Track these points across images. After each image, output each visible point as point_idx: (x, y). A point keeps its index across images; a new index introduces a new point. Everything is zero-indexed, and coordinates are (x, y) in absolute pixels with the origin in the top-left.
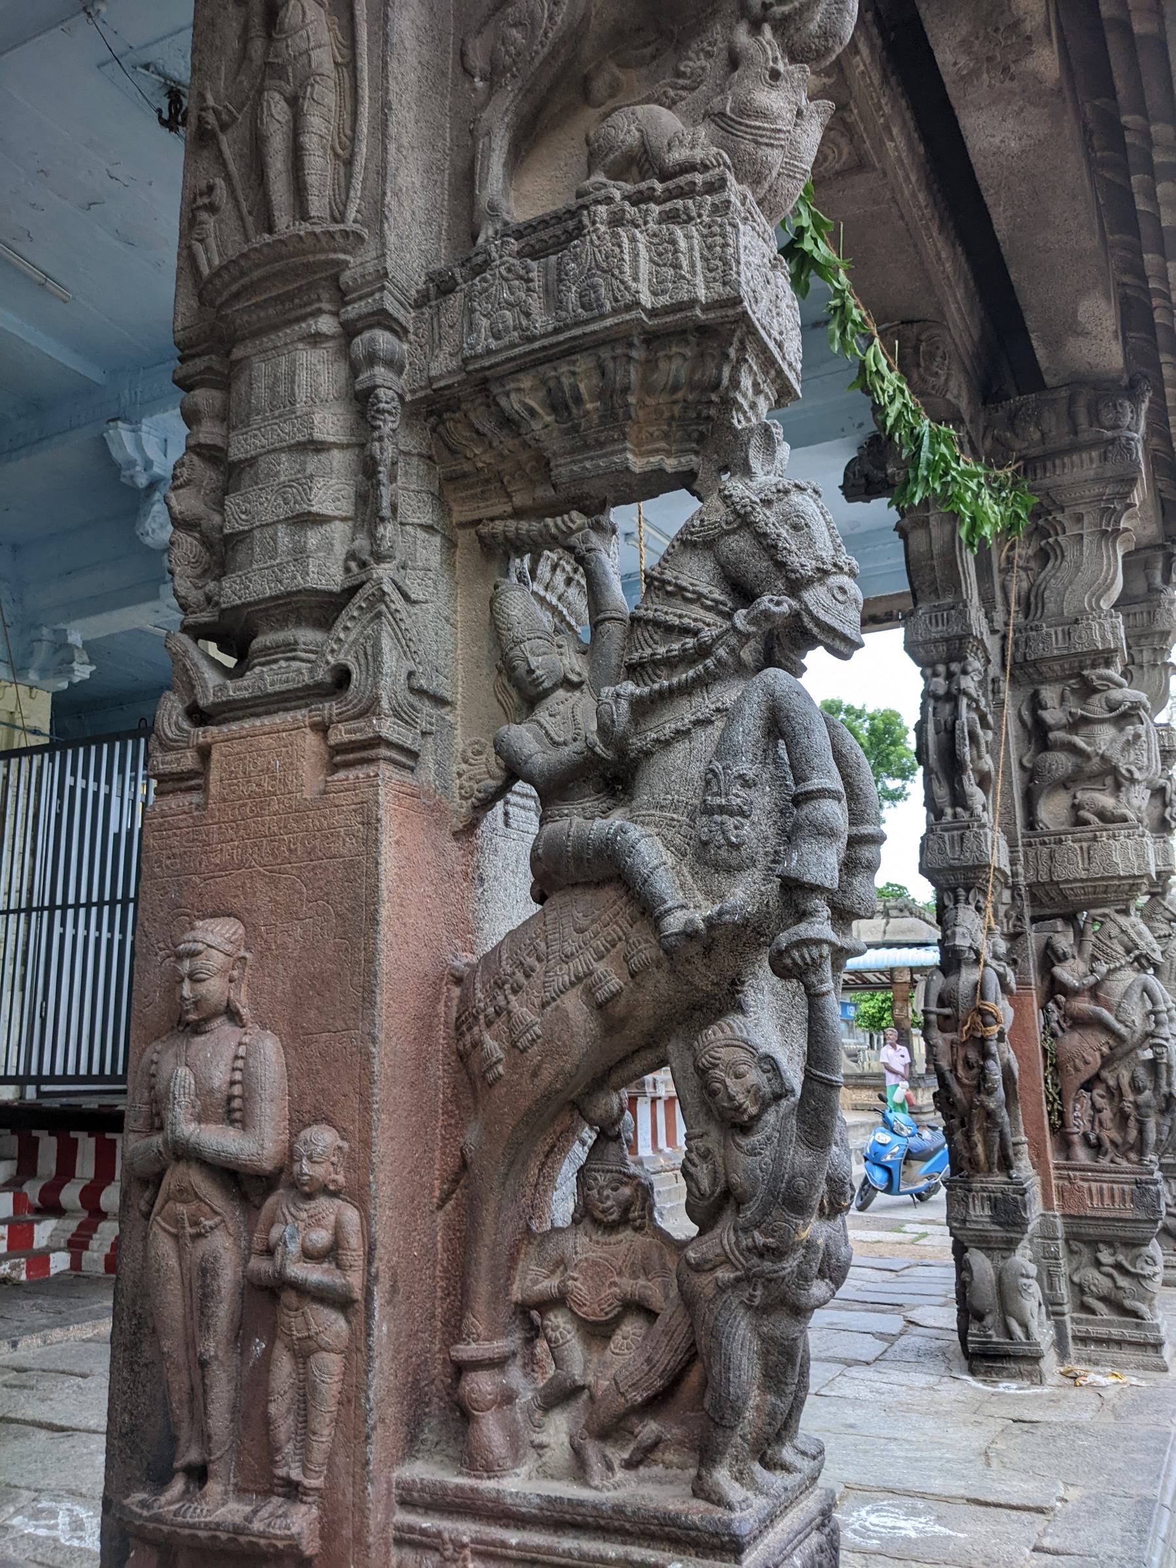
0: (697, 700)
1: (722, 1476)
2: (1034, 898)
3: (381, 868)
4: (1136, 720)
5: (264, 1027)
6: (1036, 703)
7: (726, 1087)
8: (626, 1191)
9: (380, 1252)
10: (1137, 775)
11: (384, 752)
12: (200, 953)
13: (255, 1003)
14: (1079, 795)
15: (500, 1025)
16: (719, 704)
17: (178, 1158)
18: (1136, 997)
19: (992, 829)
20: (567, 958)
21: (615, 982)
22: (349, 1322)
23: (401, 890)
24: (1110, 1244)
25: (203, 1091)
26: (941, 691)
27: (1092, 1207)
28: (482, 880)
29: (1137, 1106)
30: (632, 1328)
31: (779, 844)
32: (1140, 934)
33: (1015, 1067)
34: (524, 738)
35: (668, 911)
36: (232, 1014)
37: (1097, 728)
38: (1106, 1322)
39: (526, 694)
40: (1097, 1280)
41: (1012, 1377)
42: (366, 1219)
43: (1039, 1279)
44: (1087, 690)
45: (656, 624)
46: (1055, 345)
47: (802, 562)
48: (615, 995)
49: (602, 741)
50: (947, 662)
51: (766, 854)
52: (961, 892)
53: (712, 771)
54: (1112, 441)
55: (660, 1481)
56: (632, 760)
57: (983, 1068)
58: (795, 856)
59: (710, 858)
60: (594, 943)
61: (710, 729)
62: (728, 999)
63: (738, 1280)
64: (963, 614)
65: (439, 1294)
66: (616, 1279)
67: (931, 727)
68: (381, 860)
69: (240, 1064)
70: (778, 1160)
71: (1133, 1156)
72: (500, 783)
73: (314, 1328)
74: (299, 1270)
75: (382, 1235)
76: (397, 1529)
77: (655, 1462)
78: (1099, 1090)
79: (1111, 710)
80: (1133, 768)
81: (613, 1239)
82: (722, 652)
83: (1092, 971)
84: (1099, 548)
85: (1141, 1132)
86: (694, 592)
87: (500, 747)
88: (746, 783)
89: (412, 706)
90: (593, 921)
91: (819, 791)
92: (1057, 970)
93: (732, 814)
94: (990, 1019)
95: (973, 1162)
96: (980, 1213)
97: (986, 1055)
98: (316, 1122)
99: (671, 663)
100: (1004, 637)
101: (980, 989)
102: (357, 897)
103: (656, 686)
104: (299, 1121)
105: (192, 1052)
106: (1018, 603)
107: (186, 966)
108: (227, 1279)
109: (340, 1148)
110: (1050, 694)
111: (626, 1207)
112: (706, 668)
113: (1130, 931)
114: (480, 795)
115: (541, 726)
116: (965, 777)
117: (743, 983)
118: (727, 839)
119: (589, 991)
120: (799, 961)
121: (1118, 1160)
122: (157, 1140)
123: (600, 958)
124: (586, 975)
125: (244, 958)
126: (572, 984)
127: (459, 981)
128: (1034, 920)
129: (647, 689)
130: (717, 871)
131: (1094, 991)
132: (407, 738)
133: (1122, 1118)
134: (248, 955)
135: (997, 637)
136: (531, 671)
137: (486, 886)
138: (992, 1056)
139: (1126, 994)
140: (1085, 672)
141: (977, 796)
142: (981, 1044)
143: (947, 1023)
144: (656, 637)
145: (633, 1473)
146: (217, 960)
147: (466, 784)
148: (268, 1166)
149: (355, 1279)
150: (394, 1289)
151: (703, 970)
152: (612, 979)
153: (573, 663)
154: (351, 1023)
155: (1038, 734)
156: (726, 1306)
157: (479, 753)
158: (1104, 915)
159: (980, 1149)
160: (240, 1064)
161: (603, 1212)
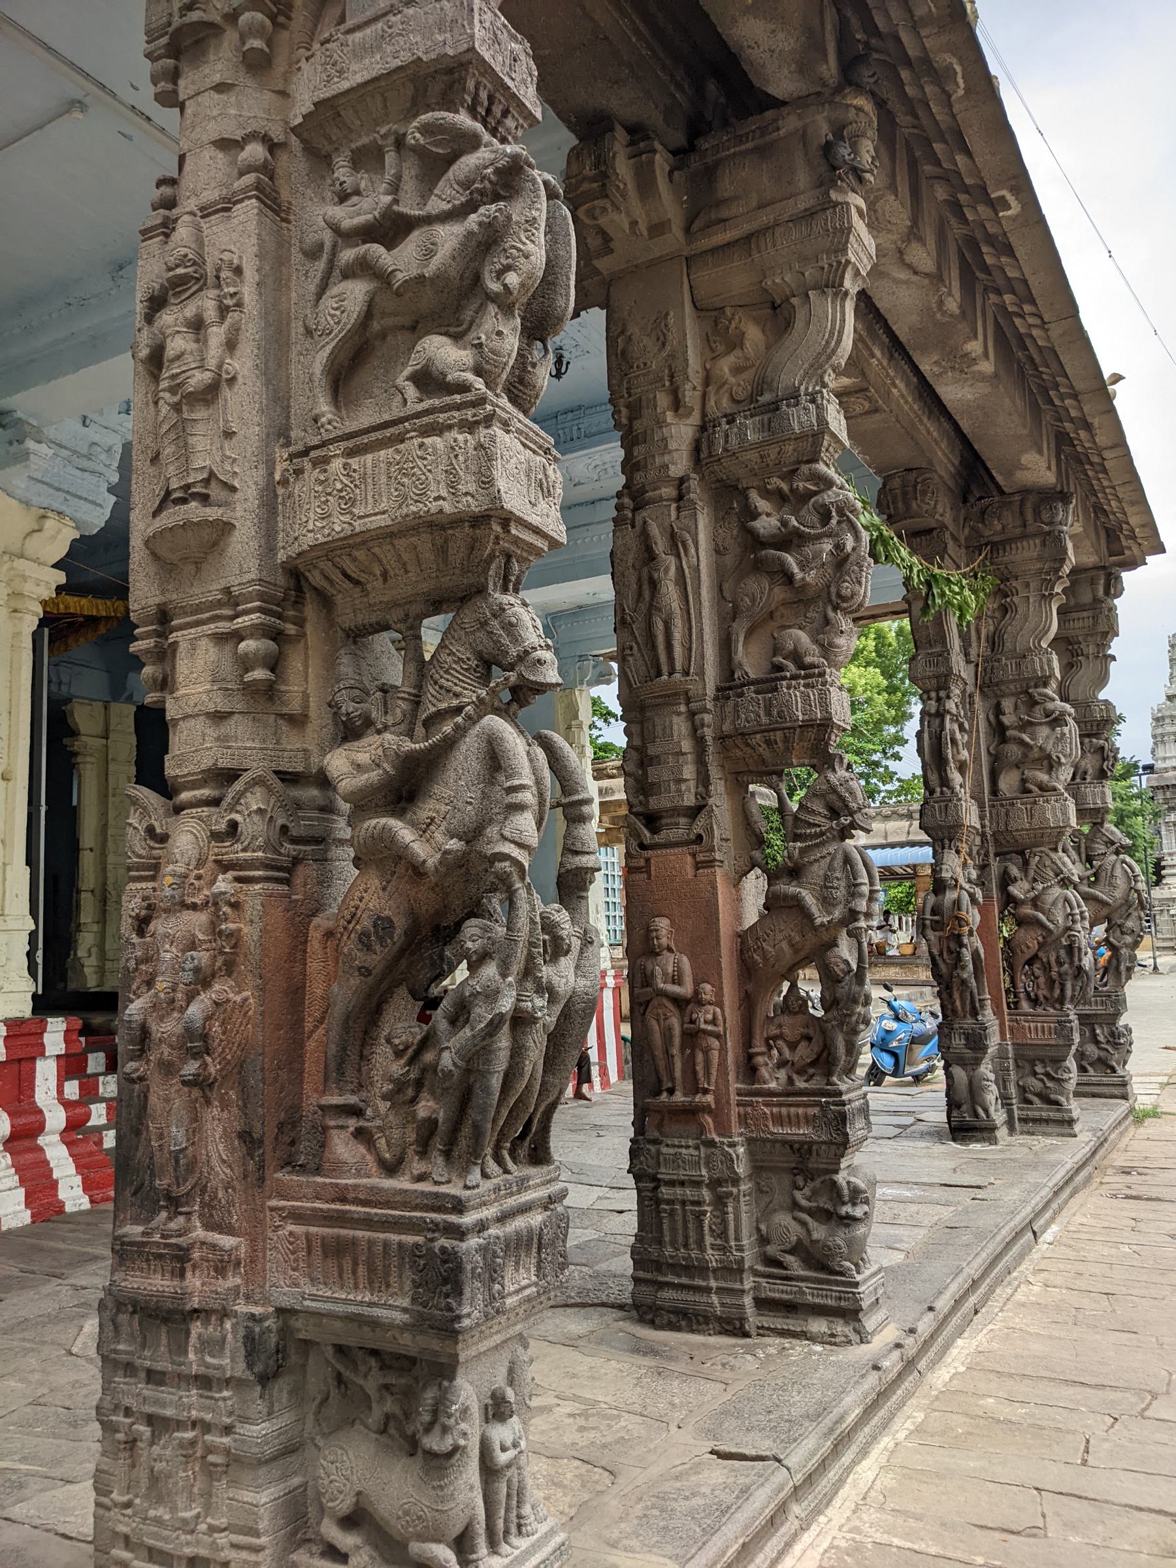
2: (996, 841)
6: (998, 711)
18: (1060, 905)
24: (1042, 1061)
26: (933, 711)
27: (1032, 1038)
29: (1060, 974)
32: (1064, 864)
33: (982, 951)
36: (670, 949)
37: (1038, 728)
38: (1039, 1109)
40: (1034, 1083)
41: (978, 1141)
46: (1009, 474)
47: (853, 805)
50: (937, 690)
52: (947, 842)
57: (959, 953)
59: (827, 902)
62: (834, 944)
64: (947, 660)
67: (926, 735)
74: (703, 1026)
78: (1037, 965)
85: (1062, 990)
92: (1011, 888)
95: (954, 1011)
96: (958, 1042)
97: (961, 945)
101: (957, 903)
104: (697, 983)
108: (677, 1031)
122: (649, 989)
128: (996, 855)
131: (1035, 902)
133: (1051, 983)
139: (1054, 903)
141: (956, 777)
142: (958, 938)
143: (937, 926)
146: (664, 932)
149: (721, 1029)
155: (999, 731)
159: (958, 1003)
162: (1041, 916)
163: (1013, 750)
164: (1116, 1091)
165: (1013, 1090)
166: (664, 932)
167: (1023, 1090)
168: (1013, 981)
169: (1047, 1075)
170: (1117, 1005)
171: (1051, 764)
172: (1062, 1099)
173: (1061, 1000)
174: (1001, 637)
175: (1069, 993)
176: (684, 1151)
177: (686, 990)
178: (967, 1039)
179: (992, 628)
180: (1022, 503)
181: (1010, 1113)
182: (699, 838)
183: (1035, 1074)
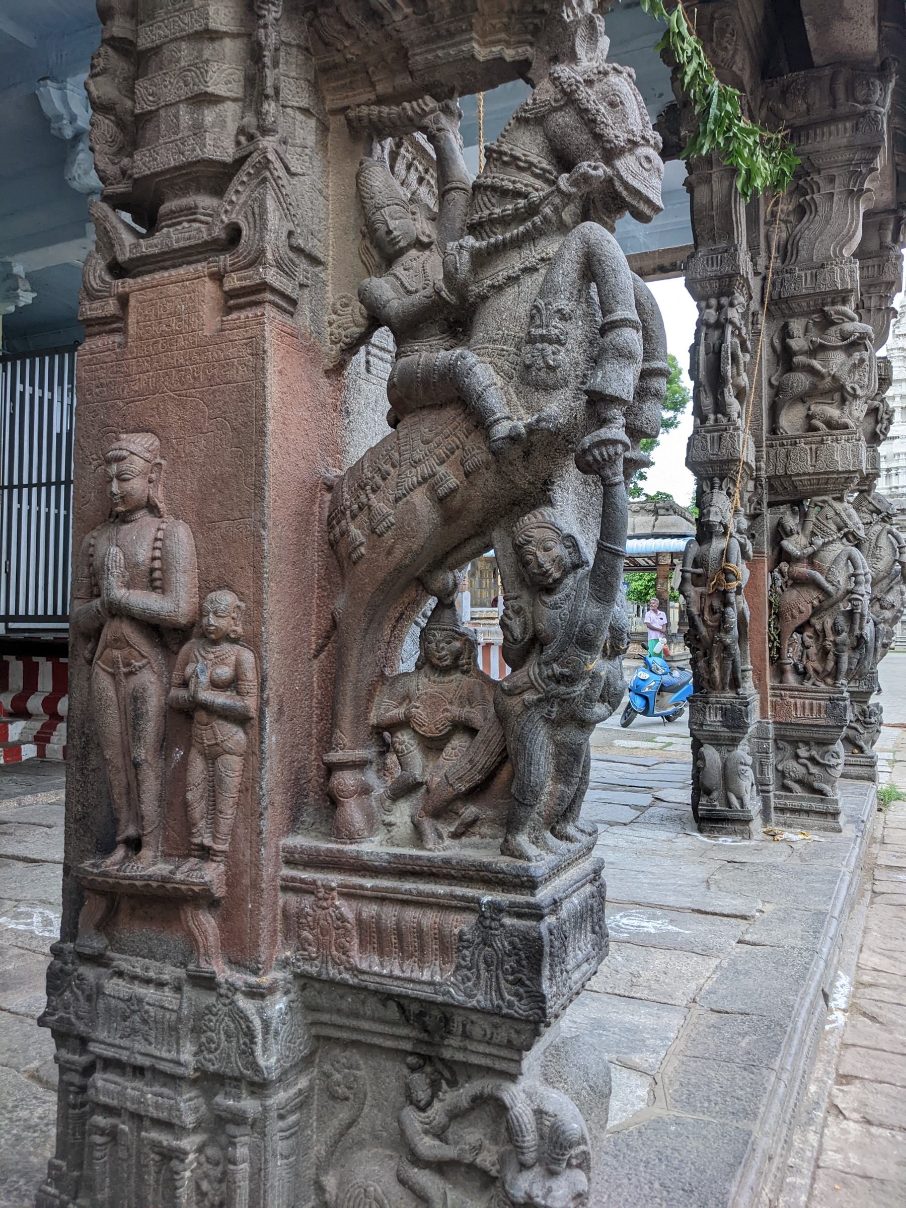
0: (525, 252)
1: (523, 840)
2: (771, 487)
3: (268, 391)
4: (862, 347)
5: (177, 517)
6: (785, 333)
7: (537, 558)
8: (457, 644)
9: (270, 683)
10: (859, 392)
11: (268, 296)
12: (125, 458)
13: (169, 500)
14: (812, 407)
15: (363, 517)
16: (544, 255)
17: (113, 616)
18: (842, 564)
19: (744, 432)
20: (416, 463)
21: (453, 481)
22: (246, 733)
23: (283, 411)
25: (131, 564)
26: (712, 320)
27: (797, 716)
28: (348, 412)
29: (835, 644)
30: (459, 742)
31: (587, 369)
32: (849, 516)
33: (748, 614)
34: (383, 288)
35: (497, 421)
36: (152, 508)
37: (832, 354)
39: (385, 252)
42: (259, 658)
44: (827, 322)
45: (494, 189)
47: (616, 134)
48: (453, 491)
49: (447, 287)
50: (718, 296)
51: (577, 376)
52: (717, 480)
53: (536, 307)
55: (476, 846)
56: (471, 305)
57: (723, 614)
58: (600, 374)
59: (532, 379)
60: (437, 451)
61: (535, 276)
62: (541, 495)
63: (540, 700)
64: (734, 257)
65: (315, 719)
66: (449, 707)
67: (702, 349)
68: (267, 384)
69: (159, 544)
70: (574, 611)
71: (829, 681)
72: (363, 330)
73: (220, 738)
74: (207, 695)
75: (273, 672)
76: (283, 880)
77: (474, 834)
78: (808, 633)
79: (844, 339)
80: (856, 386)
81: (447, 679)
82: (547, 210)
85: (837, 663)
86: (526, 162)
87: (363, 297)
88: (564, 317)
89: (291, 260)
90: (437, 434)
91: (622, 320)
92: (785, 543)
93: (550, 342)
94: (731, 577)
95: (711, 683)
96: (713, 719)
97: (726, 603)
98: (219, 588)
99: (505, 222)
101: (725, 554)
102: (248, 414)
103: (492, 240)
104: (206, 586)
105: (121, 535)
107: (114, 469)
108: (153, 704)
109: (238, 607)
110: (796, 326)
111: (457, 656)
112: (534, 224)
113: (843, 514)
114: (347, 340)
115: (397, 278)
116: (726, 390)
117: (553, 483)
118: (546, 363)
119: (433, 489)
120: (599, 458)
121: (818, 683)
122: (97, 602)
123: (442, 462)
124: (431, 476)
125: (160, 464)
126: (419, 483)
127: (330, 488)
128: (770, 505)
129: (484, 243)
130: (537, 390)
131: (811, 559)
132: (287, 286)
133: (824, 653)
134: (163, 462)
135: (759, 278)
136: (389, 232)
137: (351, 417)
138: (731, 604)
139: (835, 562)
140: (826, 308)
141: (735, 406)
142: (724, 597)
143: (698, 580)
144: (494, 201)
145: (457, 841)
146: (138, 464)
147: (336, 331)
148: (183, 621)
149: (251, 703)
150: (280, 711)
151: (522, 471)
152: (451, 478)
153: (423, 228)
154: (245, 513)
155: (785, 358)
156: (530, 720)
157: (346, 305)
158: (824, 502)
159: (717, 673)
160: (159, 544)
161: (439, 659)
164: (862, 771)
165: (771, 775)
166: (138, 464)
167: (782, 774)
169: (812, 759)
172: (827, 788)
173: (835, 674)
174: (796, 246)
175: (845, 666)
176: (149, 993)
177: (174, 604)
178: (724, 715)
179: (784, 235)
180: (833, 79)
181: (766, 802)
182: (234, 234)
183: (797, 757)
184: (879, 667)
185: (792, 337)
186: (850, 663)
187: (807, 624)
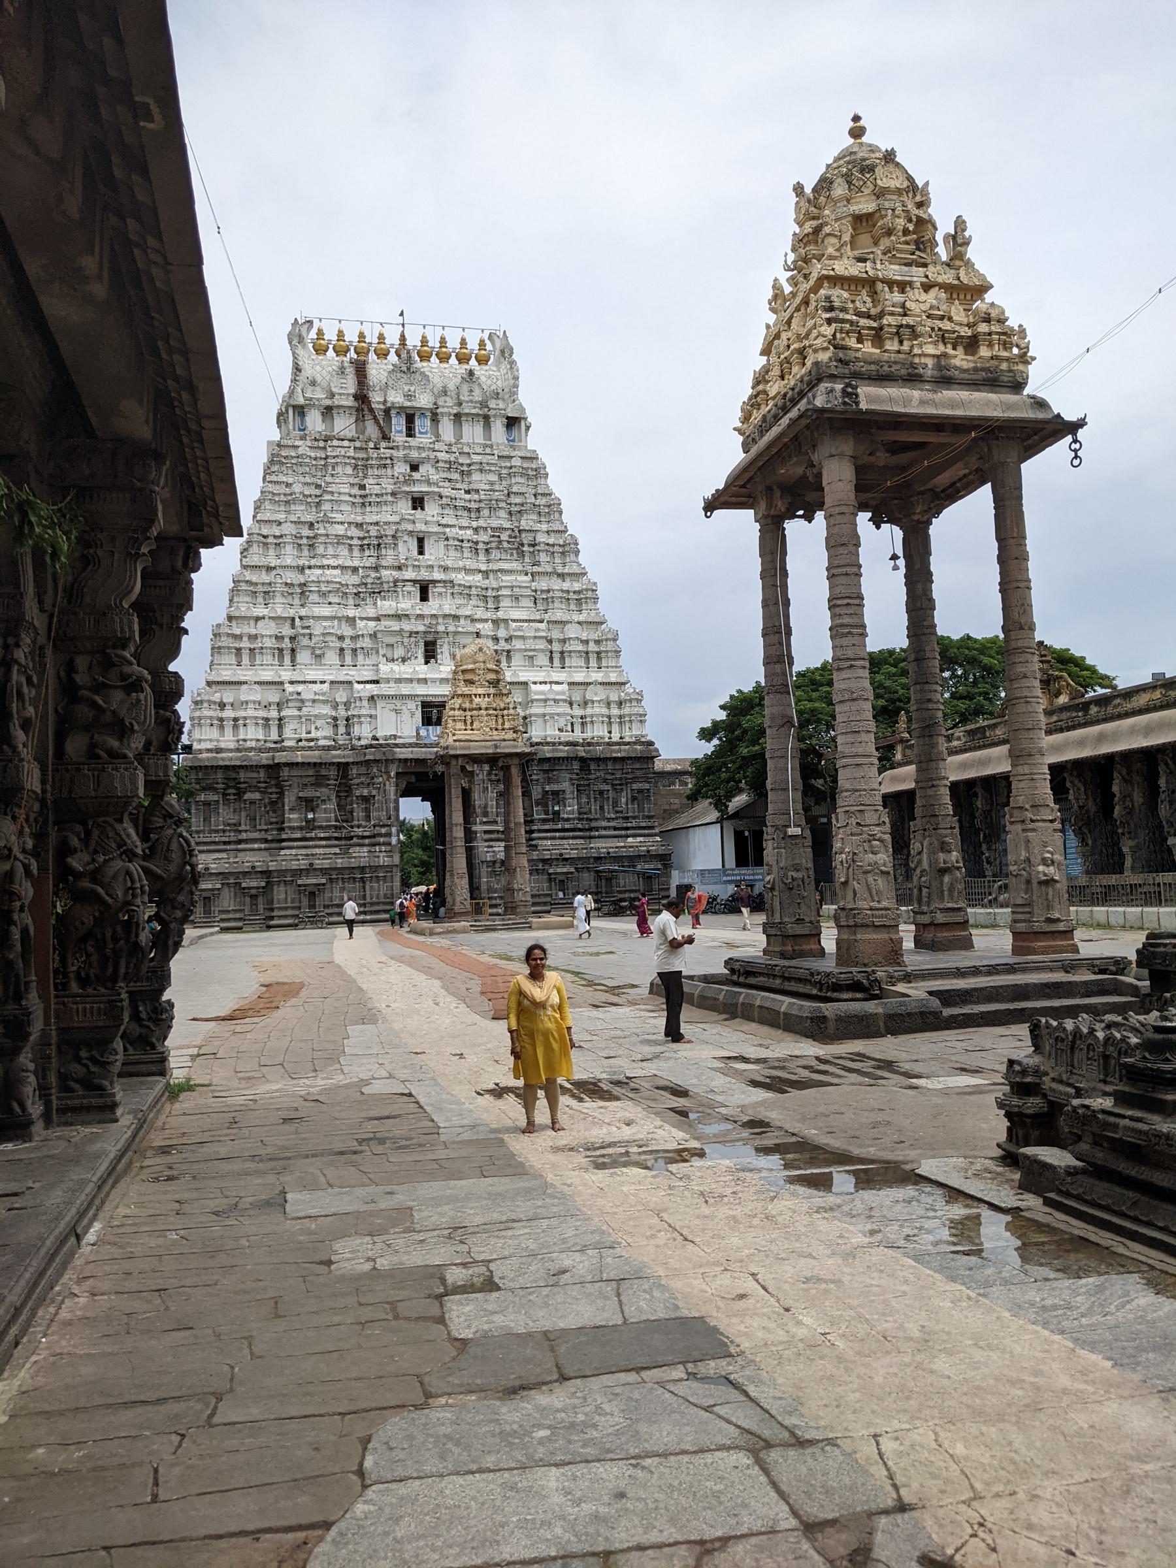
6: (71, 668)
10: (136, 727)
14: (96, 736)
18: (121, 879)
19: (29, 762)
32: (128, 835)
33: (32, 928)
43: (35, 1073)
44: (108, 664)
54: (141, 490)
64: (20, 605)
71: (109, 985)
83: (94, 860)
84: (125, 562)
94: (15, 897)
100: (51, 616)
106: (64, 591)
110: (81, 662)
113: (122, 833)
116: (11, 725)
135: (45, 615)
138: (15, 924)
139: (114, 877)
155: (69, 690)
158: (104, 822)
162: (100, 890)
163: (84, 713)
168: (63, 961)
170: (162, 979)
171: (123, 730)
173: (114, 979)
175: (122, 971)
184: (173, 964)
185: (77, 673)
186: (127, 968)
187: (89, 935)
